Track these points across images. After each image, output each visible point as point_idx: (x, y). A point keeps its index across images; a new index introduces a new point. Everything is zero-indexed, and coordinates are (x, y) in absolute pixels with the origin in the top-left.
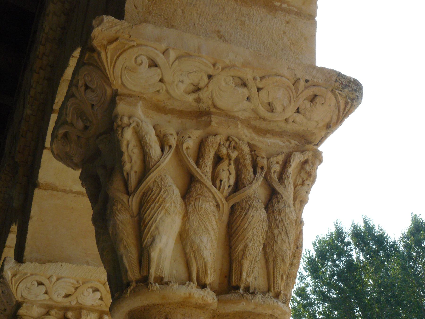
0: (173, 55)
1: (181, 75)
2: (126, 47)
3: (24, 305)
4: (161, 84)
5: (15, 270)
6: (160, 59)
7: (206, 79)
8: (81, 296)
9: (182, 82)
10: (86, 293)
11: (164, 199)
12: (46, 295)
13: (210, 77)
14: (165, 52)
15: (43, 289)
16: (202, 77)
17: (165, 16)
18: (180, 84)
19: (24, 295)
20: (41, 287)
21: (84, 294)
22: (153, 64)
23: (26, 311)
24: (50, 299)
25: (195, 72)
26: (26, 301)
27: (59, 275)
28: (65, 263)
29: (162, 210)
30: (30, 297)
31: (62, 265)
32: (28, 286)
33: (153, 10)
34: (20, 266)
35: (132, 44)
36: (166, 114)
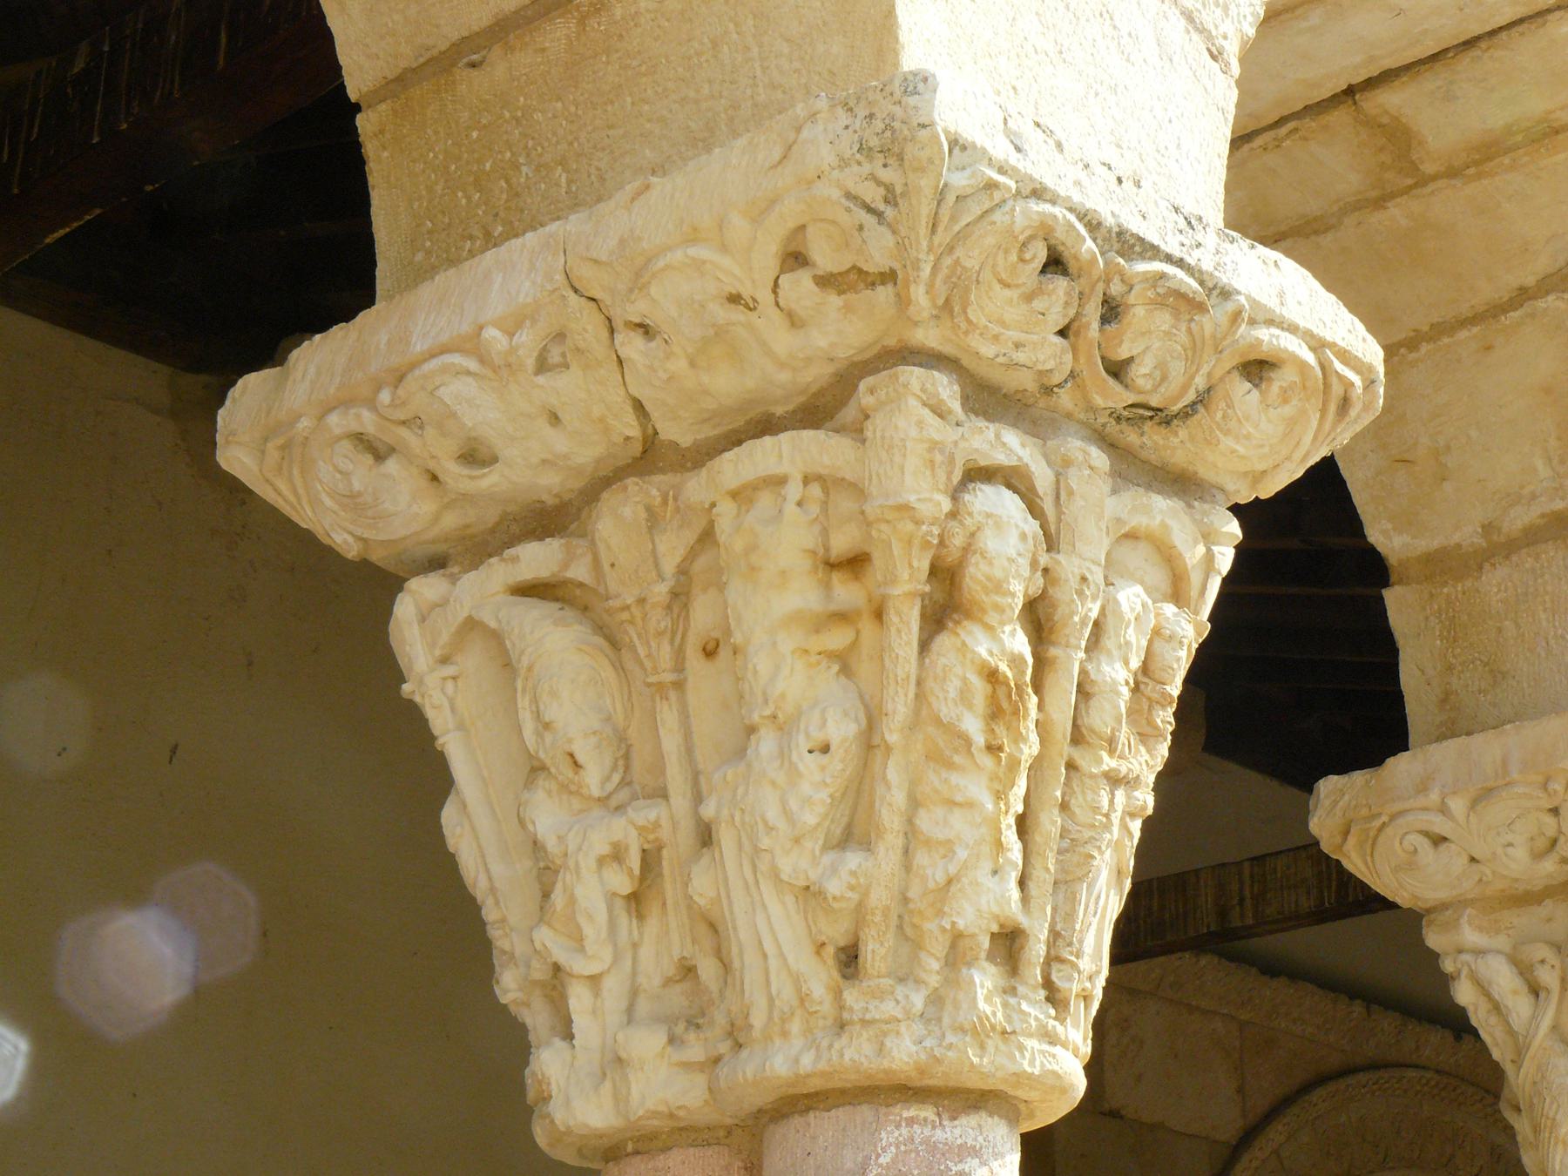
0: (1458, 805)
1: (1498, 834)
2: (1372, 834)
4: (1475, 866)
6: (1440, 825)
7: (1549, 820)
9: (1510, 845)
11: (1554, 1119)
13: (1555, 811)
14: (1444, 810)
16: (1537, 819)
17: (1482, 658)
18: (1510, 850)
22: (1438, 840)
25: (1518, 817)
29: (1556, 1144)
33: (1454, 656)
35: (1377, 823)
36: (1539, 903)
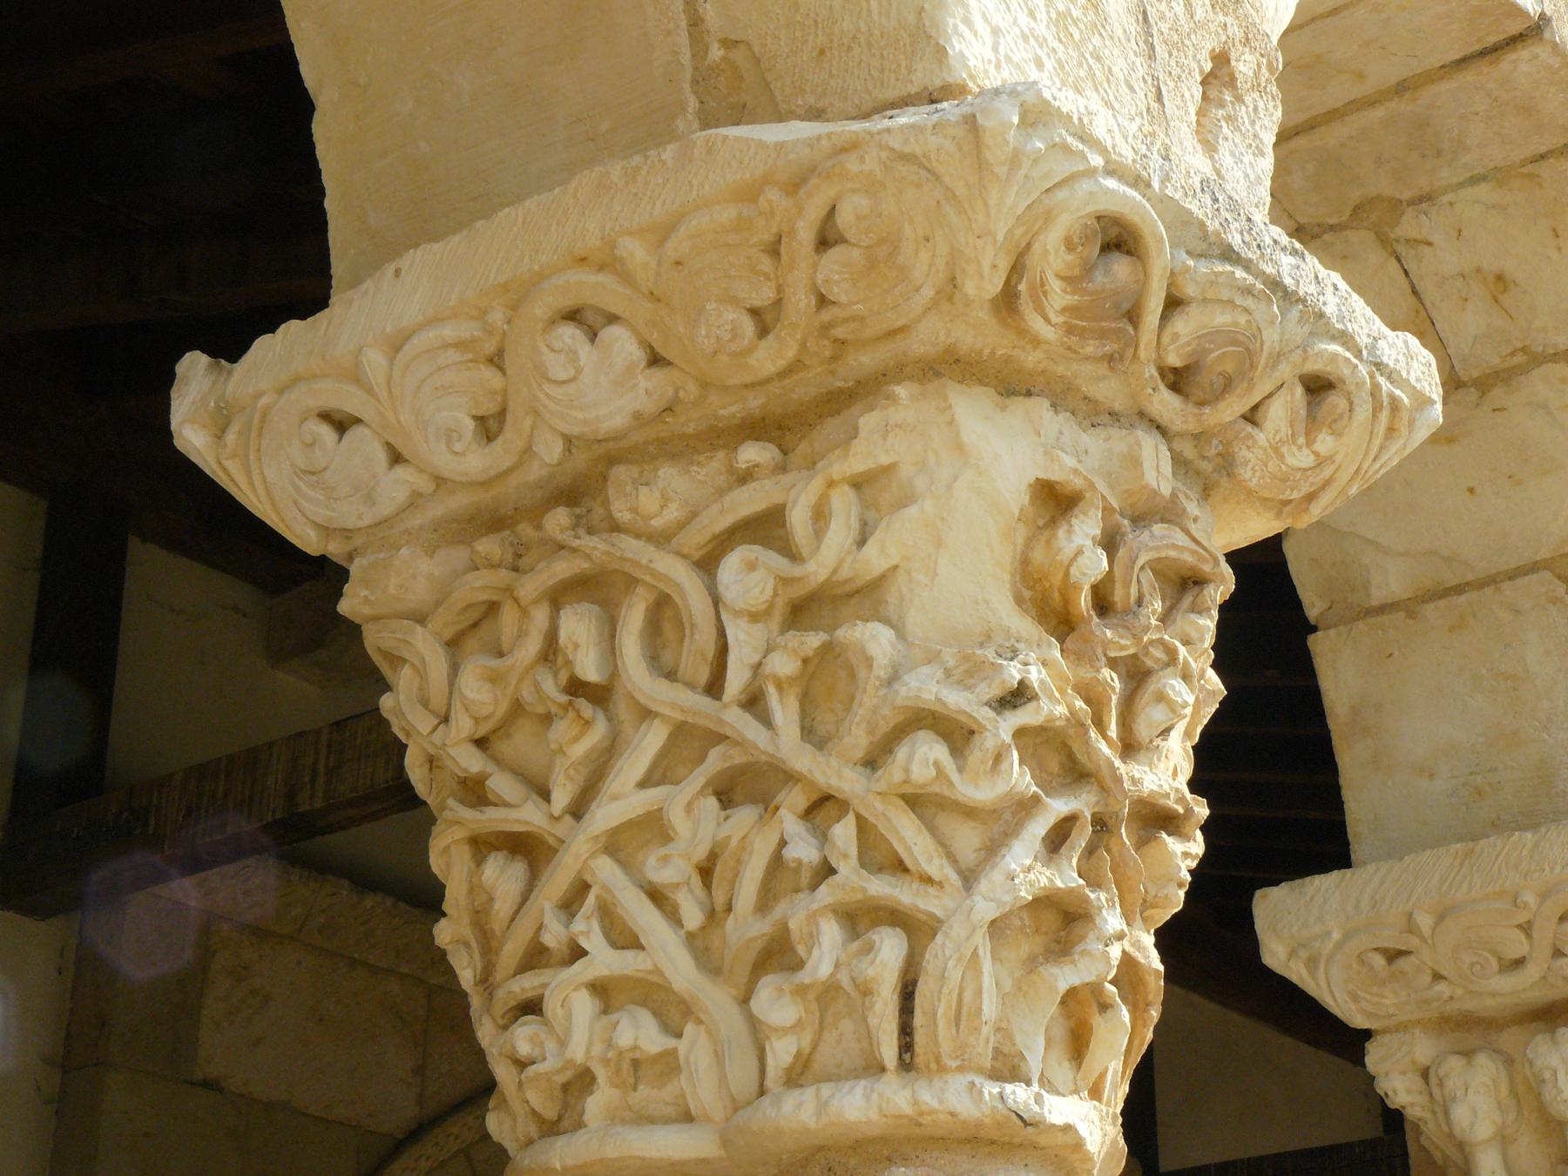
3: (354, 570)
5: (212, 404)
8: (548, 396)
10: (557, 368)
12: (400, 471)
15: (365, 446)
19: (320, 514)
20: (353, 434)
21: (554, 378)
23: (364, 593)
24: (440, 481)
26: (358, 541)
27: (388, 330)
28: (411, 251)
30: (353, 514)
31: (397, 272)
32: (301, 462)
34: (230, 373)
